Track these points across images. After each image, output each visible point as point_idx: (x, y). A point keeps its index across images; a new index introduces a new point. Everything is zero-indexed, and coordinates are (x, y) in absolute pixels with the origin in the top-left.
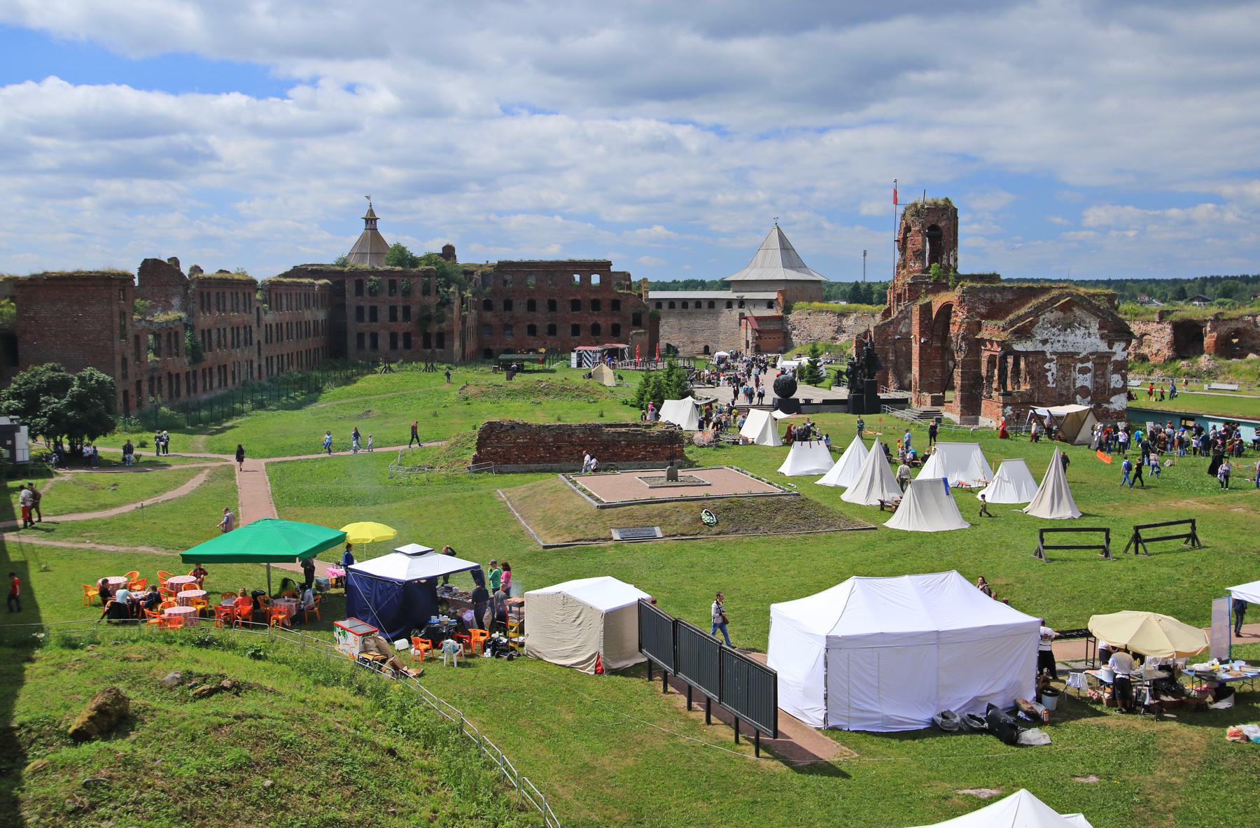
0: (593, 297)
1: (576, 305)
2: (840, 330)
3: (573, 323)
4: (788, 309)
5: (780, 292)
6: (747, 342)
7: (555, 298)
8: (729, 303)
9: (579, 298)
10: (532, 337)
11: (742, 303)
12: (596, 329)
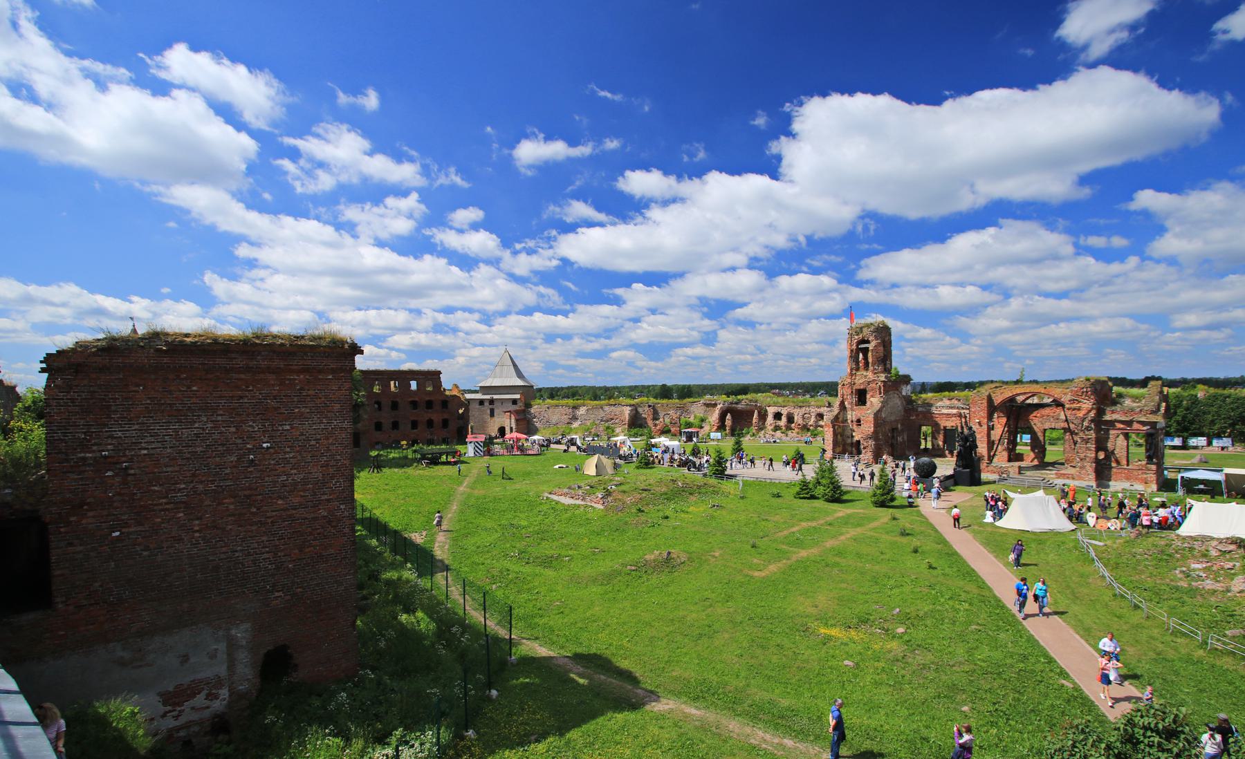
0: (427, 399)
1: (414, 404)
2: (575, 418)
3: (412, 418)
4: (529, 406)
5: (521, 394)
6: (511, 429)
7: (398, 400)
8: (481, 402)
9: (417, 399)
10: (379, 432)
11: (492, 402)
12: (430, 423)
